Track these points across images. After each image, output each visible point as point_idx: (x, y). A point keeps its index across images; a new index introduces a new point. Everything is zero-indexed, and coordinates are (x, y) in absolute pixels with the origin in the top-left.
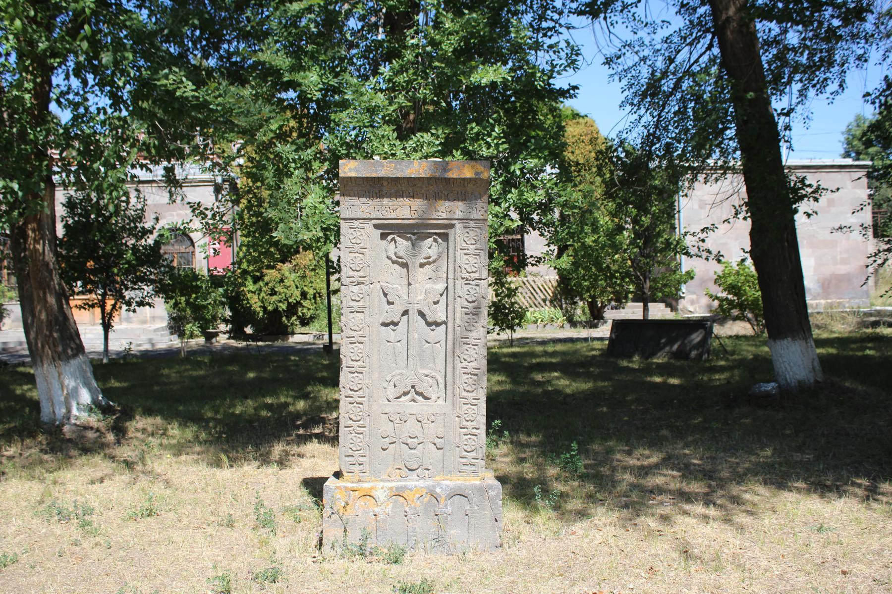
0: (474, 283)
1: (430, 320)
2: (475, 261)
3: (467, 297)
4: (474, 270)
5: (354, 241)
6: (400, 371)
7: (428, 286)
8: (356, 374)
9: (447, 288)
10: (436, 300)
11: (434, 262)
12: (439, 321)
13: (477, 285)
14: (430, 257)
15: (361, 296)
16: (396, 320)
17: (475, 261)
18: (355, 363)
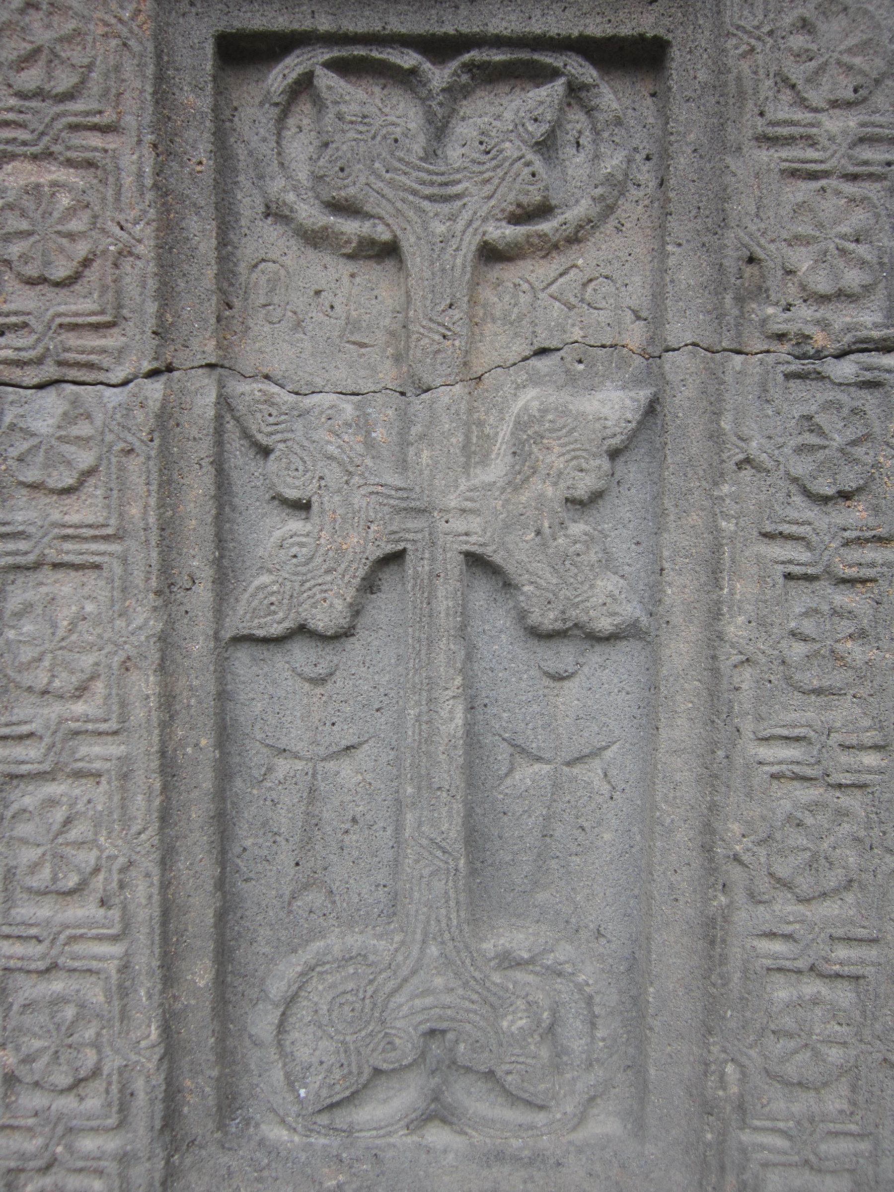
0: (846, 369)
1: (548, 620)
2: (859, 217)
3: (801, 467)
4: (853, 278)
5: (31, 78)
6: (355, 941)
7: (530, 397)
8: (57, 985)
9: (652, 409)
10: (584, 485)
11: (573, 240)
12: (605, 624)
13: (872, 385)
14: (544, 210)
15: (85, 458)
16: (321, 621)
17: (859, 217)
18: (44, 910)
